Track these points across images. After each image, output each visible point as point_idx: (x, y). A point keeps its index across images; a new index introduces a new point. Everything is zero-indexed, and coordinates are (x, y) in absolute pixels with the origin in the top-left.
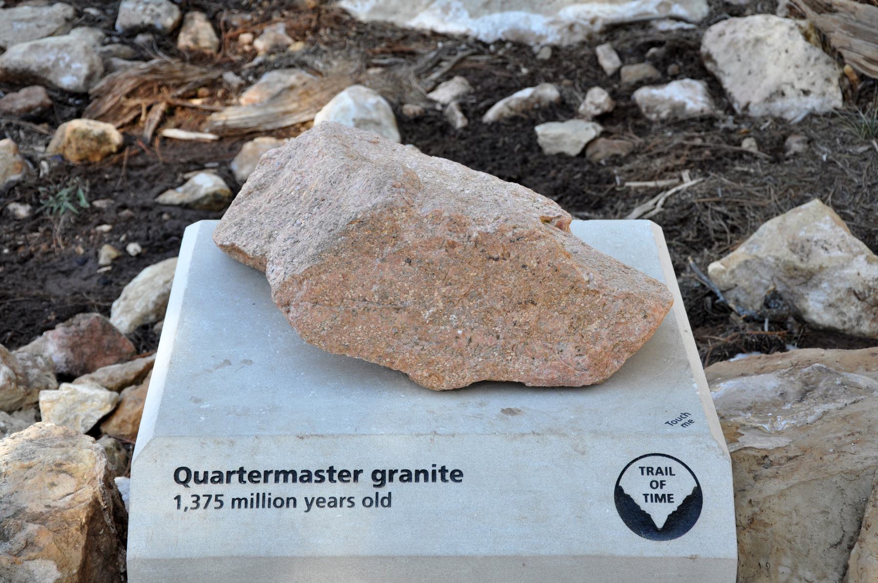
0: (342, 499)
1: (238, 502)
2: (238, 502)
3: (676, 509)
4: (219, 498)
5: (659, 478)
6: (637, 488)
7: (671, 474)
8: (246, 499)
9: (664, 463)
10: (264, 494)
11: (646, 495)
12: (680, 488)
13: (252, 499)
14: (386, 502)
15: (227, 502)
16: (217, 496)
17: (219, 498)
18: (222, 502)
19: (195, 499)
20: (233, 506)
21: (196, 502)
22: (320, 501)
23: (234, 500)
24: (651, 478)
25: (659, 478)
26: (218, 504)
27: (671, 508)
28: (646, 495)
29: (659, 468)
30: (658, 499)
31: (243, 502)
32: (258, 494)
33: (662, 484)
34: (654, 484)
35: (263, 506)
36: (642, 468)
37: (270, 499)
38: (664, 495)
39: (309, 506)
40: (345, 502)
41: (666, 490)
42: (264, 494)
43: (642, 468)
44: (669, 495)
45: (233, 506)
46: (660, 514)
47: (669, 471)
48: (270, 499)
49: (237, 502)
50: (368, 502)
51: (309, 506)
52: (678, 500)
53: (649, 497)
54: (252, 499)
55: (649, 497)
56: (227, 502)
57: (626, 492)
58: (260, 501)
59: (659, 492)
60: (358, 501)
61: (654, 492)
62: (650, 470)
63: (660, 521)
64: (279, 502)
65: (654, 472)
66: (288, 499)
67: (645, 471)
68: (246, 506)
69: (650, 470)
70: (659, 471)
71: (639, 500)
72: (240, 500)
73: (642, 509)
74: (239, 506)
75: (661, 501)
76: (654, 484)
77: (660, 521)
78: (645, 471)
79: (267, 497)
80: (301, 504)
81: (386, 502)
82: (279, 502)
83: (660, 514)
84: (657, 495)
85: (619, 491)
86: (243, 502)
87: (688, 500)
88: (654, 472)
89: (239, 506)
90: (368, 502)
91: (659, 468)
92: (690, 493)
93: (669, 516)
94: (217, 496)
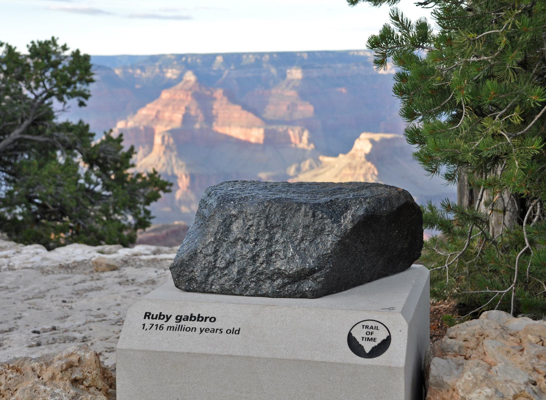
0: (217, 330)
5: (371, 330)
6: (359, 334)
11: (363, 338)
12: (380, 336)
14: (237, 332)
22: (207, 330)
24: (367, 330)
25: (371, 330)
28: (363, 338)
34: (368, 333)
36: (363, 326)
38: (372, 339)
39: (201, 331)
40: (218, 331)
43: (363, 326)
46: (368, 347)
47: (377, 328)
50: (229, 332)
51: (201, 331)
53: (364, 339)
55: (364, 339)
59: (370, 337)
60: (224, 331)
61: (367, 336)
62: (367, 327)
64: (188, 329)
66: (193, 328)
67: (365, 327)
69: (367, 327)
70: (372, 327)
72: (171, 327)
76: (368, 333)
77: (367, 350)
78: (365, 327)
80: (198, 331)
81: (237, 332)
82: (188, 329)
84: (368, 338)
85: (350, 335)
90: (229, 332)
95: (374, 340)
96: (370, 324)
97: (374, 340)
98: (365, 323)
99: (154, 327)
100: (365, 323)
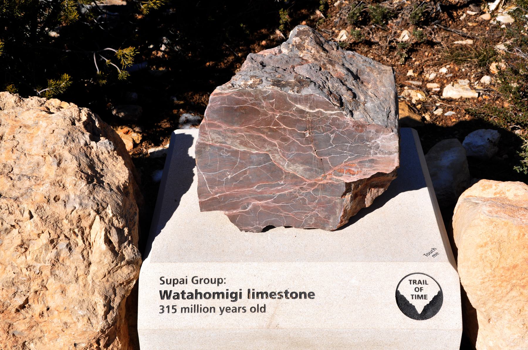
1: (184, 309)
2: (184, 309)
3: (428, 303)
4: (174, 307)
5: (420, 286)
6: (407, 291)
7: (426, 284)
8: (188, 308)
9: (422, 278)
10: (198, 305)
11: (412, 295)
12: (431, 292)
13: (192, 308)
15: (179, 310)
16: (173, 306)
17: (174, 307)
18: (176, 310)
19: (162, 308)
20: (182, 312)
21: (162, 309)
23: (182, 309)
25: (420, 286)
26: (174, 311)
27: (427, 302)
28: (412, 295)
29: (420, 281)
30: (418, 297)
31: (187, 309)
32: (195, 305)
33: (421, 289)
34: (417, 290)
35: (198, 312)
36: (410, 281)
37: (201, 308)
38: (422, 296)
41: (423, 293)
42: (198, 305)
43: (410, 281)
44: (425, 295)
45: (182, 312)
46: (419, 306)
48: (201, 308)
49: (184, 309)
52: (430, 299)
53: (414, 296)
54: (192, 308)
55: (414, 296)
56: (179, 310)
57: (402, 293)
58: (197, 309)
59: (420, 293)
61: (417, 294)
62: (415, 282)
63: (420, 310)
65: (417, 282)
67: (412, 282)
68: (188, 312)
69: (415, 282)
71: (409, 298)
72: (185, 309)
73: (410, 303)
74: (185, 312)
75: (420, 299)
76: (417, 290)
77: (420, 310)
78: (412, 282)
79: (200, 307)
82: (206, 310)
83: (419, 306)
84: (418, 296)
85: (397, 292)
86: (187, 309)
87: (435, 298)
88: (417, 282)
89: (185, 312)
91: (420, 281)
92: (437, 294)
93: (425, 306)
94: (173, 306)
95: (425, 297)
96: (417, 277)
97: (425, 297)
98: (412, 277)
99: (166, 309)
100: (412, 277)
